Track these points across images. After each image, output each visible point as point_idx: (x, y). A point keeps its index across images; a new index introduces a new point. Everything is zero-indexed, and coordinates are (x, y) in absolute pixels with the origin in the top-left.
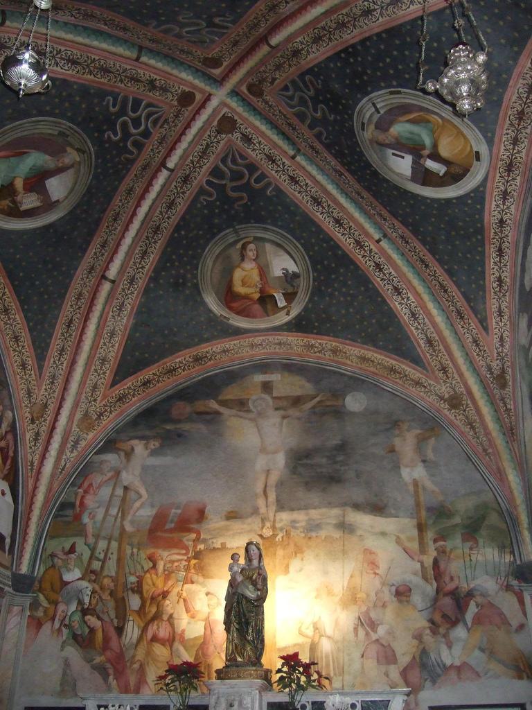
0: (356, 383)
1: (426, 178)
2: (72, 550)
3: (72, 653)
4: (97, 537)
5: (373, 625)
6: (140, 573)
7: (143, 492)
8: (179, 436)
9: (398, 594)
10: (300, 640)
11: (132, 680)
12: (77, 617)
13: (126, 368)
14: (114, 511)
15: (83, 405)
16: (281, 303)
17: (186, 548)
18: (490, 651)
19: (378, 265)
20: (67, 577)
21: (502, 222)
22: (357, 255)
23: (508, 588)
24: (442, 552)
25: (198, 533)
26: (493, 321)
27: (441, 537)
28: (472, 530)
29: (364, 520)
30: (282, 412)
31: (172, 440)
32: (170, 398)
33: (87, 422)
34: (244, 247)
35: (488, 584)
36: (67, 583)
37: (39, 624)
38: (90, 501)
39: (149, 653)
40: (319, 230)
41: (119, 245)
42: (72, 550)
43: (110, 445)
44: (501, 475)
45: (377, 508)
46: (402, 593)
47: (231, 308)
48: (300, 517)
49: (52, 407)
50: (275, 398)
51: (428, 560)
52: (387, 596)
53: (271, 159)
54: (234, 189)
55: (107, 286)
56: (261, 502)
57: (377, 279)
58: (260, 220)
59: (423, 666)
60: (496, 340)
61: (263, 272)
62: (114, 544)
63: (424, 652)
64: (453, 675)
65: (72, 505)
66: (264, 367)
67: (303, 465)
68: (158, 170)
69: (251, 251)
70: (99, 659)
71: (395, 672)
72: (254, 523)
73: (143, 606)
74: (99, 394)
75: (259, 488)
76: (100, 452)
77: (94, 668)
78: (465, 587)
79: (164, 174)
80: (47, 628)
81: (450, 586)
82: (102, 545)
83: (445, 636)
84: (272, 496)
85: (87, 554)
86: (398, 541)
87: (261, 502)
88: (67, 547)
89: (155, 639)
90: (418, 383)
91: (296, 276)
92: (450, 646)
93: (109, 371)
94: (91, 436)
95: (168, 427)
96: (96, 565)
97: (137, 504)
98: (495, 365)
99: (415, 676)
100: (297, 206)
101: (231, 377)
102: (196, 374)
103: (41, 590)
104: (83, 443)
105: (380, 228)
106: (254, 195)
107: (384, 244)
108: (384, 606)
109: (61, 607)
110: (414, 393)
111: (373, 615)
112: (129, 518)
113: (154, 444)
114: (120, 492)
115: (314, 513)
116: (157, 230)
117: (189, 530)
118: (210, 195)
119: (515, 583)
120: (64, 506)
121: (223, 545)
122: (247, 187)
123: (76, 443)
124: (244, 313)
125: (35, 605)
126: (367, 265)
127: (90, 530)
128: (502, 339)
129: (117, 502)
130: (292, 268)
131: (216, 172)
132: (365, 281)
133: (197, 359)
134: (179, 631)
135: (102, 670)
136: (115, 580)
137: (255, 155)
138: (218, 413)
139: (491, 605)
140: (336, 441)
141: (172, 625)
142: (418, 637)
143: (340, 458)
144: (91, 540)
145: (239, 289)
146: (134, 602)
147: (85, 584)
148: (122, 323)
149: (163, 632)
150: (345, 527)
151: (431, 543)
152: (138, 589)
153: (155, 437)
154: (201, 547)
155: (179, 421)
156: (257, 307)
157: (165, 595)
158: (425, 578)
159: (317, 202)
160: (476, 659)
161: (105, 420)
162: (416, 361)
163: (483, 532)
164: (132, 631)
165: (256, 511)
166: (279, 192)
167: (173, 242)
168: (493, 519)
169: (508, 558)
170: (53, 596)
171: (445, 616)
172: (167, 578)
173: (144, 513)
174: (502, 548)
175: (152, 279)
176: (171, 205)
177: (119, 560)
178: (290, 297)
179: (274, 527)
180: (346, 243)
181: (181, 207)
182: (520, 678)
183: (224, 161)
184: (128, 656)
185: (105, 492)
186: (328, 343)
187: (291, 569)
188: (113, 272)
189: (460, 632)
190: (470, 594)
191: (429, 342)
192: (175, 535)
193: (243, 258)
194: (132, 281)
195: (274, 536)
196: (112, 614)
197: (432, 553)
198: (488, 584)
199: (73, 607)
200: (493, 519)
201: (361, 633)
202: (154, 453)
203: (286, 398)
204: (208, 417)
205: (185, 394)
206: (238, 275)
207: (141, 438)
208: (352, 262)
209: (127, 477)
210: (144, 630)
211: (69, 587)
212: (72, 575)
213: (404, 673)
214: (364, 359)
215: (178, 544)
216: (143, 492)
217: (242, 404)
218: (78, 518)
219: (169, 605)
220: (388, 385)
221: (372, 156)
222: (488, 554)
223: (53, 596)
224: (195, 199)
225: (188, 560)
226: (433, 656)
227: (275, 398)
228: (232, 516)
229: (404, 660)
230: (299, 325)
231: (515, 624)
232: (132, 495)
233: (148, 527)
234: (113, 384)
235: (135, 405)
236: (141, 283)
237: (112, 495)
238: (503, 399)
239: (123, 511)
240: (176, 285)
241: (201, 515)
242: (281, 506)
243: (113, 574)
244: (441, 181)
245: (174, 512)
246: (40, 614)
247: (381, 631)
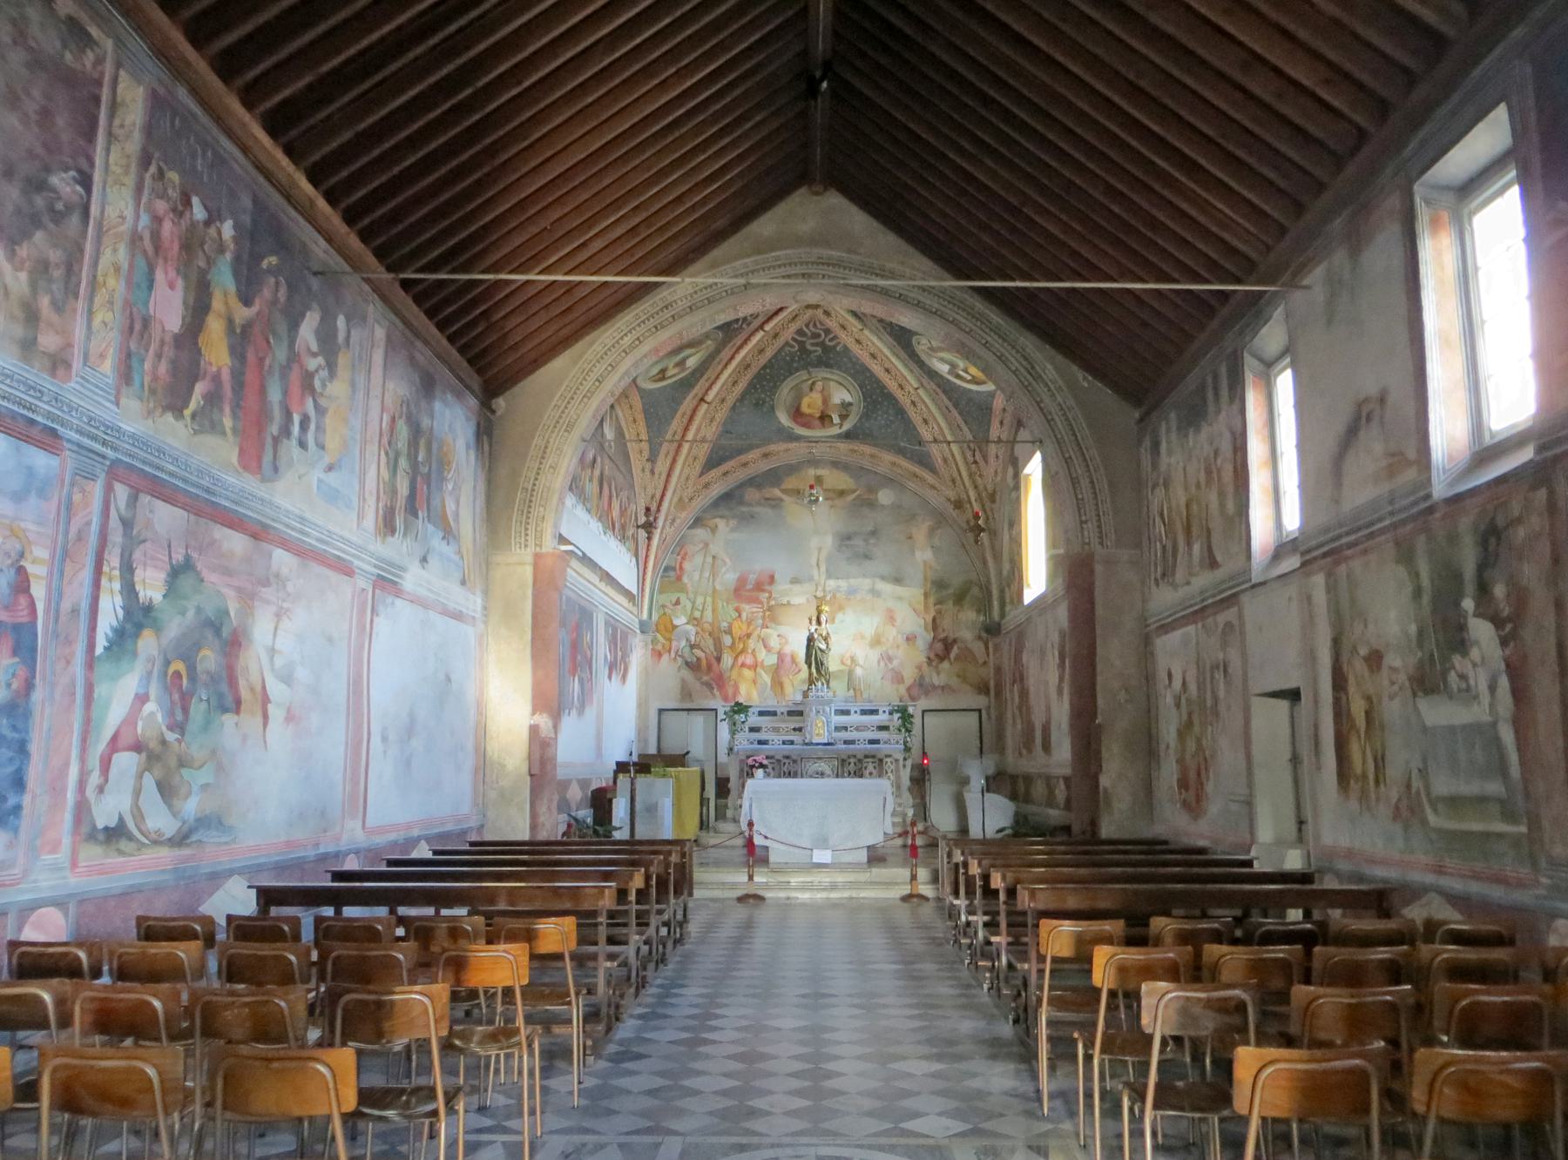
0: (889, 481)
1: (958, 376)
2: (678, 603)
3: (686, 673)
4: (696, 594)
5: (890, 659)
6: (730, 620)
7: (728, 560)
8: (752, 517)
9: (908, 639)
10: (842, 667)
11: (730, 691)
12: (688, 649)
13: (712, 463)
14: (707, 574)
15: (678, 492)
16: (836, 420)
17: (761, 603)
18: (962, 677)
19: (913, 403)
20: (677, 622)
21: (1004, 410)
22: (898, 394)
23: (980, 638)
24: (939, 612)
25: (770, 593)
26: (992, 460)
27: (939, 602)
28: (959, 599)
29: (886, 588)
30: (830, 502)
31: (748, 519)
32: (742, 486)
33: (681, 504)
34: (814, 383)
35: (967, 635)
36: (676, 627)
37: (660, 655)
38: (687, 566)
39: (740, 675)
40: (873, 375)
41: (717, 378)
42: (678, 603)
43: (698, 522)
44: (985, 562)
45: (898, 580)
46: (910, 639)
47: (797, 422)
48: (843, 584)
49: (658, 496)
50: (826, 490)
51: (929, 619)
52: (901, 640)
53: (843, 327)
54: (813, 345)
55: (704, 407)
56: (815, 573)
57: (911, 412)
58: (828, 366)
59: (921, 685)
60: (992, 470)
61: (825, 401)
62: (709, 600)
63: (922, 677)
64: (940, 691)
65: (674, 569)
66: (814, 462)
67: (847, 546)
68: (757, 330)
69: (819, 385)
70: (705, 678)
71: (902, 689)
72: (808, 587)
73: (733, 643)
74: (690, 482)
75: (814, 562)
76: (689, 528)
77: (703, 683)
78: (952, 636)
79: (760, 334)
80: (665, 657)
81: (942, 636)
82: (700, 600)
83: (936, 667)
84: (823, 569)
85: (689, 606)
86: (910, 605)
87: (815, 573)
88: (674, 601)
89: (743, 665)
90: (933, 487)
91: (850, 404)
92: (938, 674)
93: (698, 467)
94: (683, 515)
95: (744, 509)
96: (697, 614)
97: (724, 570)
98: (990, 488)
99: (915, 692)
100: (858, 359)
101: (792, 469)
102: (764, 466)
103: (658, 631)
104: (678, 521)
105: (919, 380)
106: (826, 349)
107: (921, 392)
108: (898, 647)
109: (674, 644)
110: (930, 495)
111: (890, 652)
112: (718, 580)
113: (733, 523)
114: (709, 560)
115: (852, 581)
116: (748, 366)
117: (763, 591)
118: (792, 347)
119: (984, 635)
120: (667, 569)
121: (789, 603)
122: (822, 344)
123: (674, 520)
124: (806, 425)
125: (655, 641)
126: (904, 401)
127: (690, 589)
128: (996, 472)
129: (708, 567)
130: (848, 398)
131: (800, 332)
132: (901, 412)
133: (766, 455)
134: (759, 660)
135: (708, 685)
136: (711, 624)
137: (831, 324)
138: (781, 500)
139: (967, 648)
140: (870, 528)
141: (754, 656)
142: (919, 668)
143: (872, 541)
144: (691, 596)
145: (805, 409)
146: (727, 640)
147: (689, 627)
148: (711, 432)
149: (749, 660)
150: (875, 593)
151: (931, 605)
152: (729, 632)
153: (733, 518)
154: (773, 603)
155: (750, 505)
156: (817, 422)
157: (749, 636)
158: (926, 628)
159: (873, 356)
160: (955, 681)
161: (694, 503)
162: (933, 470)
163: (968, 598)
164: (727, 660)
165: (811, 579)
166: (845, 347)
167: (759, 377)
168: (975, 591)
169: (982, 618)
170: (667, 635)
171: (937, 655)
172: (749, 624)
173: (729, 577)
174: (979, 611)
175: (738, 400)
176: (761, 351)
177: (714, 611)
178: (843, 417)
179: (824, 591)
180: (892, 386)
181: (769, 353)
182: (979, 693)
183: (807, 326)
184: (726, 675)
185: (698, 559)
186: (868, 449)
187: (837, 621)
188: (709, 398)
189: (945, 665)
190: (955, 641)
191: (945, 460)
192: (755, 594)
193: (811, 390)
194: (723, 400)
195: (825, 596)
196: (712, 648)
197: (933, 613)
198: (967, 635)
199: (683, 643)
200: (975, 591)
201: (882, 664)
202: (733, 530)
203: (834, 491)
204: (773, 503)
205: (754, 482)
206: (805, 402)
207: (721, 517)
208: (895, 399)
209: (717, 547)
210: (736, 658)
211: (677, 630)
212: (680, 621)
213: (909, 689)
214: (894, 464)
215: (756, 601)
216: (728, 560)
217: (797, 493)
218: (679, 578)
219: (752, 643)
220: (911, 485)
221: (923, 357)
222: (970, 615)
223: (667, 635)
224: (782, 348)
225: (764, 612)
226: (927, 680)
227: (826, 490)
228: (795, 581)
229: (909, 681)
230: (848, 436)
231: (981, 661)
232: (719, 562)
233: (733, 587)
234: (702, 474)
235: (717, 490)
236: (731, 400)
237: (704, 562)
238: (992, 510)
239: (714, 574)
240: (757, 404)
241: (772, 579)
242: (829, 576)
243: (710, 620)
244: (968, 382)
245: (752, 578)
246: (659, 647)
247: (895, 663)
